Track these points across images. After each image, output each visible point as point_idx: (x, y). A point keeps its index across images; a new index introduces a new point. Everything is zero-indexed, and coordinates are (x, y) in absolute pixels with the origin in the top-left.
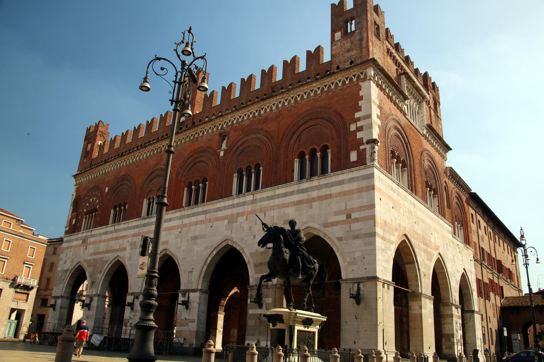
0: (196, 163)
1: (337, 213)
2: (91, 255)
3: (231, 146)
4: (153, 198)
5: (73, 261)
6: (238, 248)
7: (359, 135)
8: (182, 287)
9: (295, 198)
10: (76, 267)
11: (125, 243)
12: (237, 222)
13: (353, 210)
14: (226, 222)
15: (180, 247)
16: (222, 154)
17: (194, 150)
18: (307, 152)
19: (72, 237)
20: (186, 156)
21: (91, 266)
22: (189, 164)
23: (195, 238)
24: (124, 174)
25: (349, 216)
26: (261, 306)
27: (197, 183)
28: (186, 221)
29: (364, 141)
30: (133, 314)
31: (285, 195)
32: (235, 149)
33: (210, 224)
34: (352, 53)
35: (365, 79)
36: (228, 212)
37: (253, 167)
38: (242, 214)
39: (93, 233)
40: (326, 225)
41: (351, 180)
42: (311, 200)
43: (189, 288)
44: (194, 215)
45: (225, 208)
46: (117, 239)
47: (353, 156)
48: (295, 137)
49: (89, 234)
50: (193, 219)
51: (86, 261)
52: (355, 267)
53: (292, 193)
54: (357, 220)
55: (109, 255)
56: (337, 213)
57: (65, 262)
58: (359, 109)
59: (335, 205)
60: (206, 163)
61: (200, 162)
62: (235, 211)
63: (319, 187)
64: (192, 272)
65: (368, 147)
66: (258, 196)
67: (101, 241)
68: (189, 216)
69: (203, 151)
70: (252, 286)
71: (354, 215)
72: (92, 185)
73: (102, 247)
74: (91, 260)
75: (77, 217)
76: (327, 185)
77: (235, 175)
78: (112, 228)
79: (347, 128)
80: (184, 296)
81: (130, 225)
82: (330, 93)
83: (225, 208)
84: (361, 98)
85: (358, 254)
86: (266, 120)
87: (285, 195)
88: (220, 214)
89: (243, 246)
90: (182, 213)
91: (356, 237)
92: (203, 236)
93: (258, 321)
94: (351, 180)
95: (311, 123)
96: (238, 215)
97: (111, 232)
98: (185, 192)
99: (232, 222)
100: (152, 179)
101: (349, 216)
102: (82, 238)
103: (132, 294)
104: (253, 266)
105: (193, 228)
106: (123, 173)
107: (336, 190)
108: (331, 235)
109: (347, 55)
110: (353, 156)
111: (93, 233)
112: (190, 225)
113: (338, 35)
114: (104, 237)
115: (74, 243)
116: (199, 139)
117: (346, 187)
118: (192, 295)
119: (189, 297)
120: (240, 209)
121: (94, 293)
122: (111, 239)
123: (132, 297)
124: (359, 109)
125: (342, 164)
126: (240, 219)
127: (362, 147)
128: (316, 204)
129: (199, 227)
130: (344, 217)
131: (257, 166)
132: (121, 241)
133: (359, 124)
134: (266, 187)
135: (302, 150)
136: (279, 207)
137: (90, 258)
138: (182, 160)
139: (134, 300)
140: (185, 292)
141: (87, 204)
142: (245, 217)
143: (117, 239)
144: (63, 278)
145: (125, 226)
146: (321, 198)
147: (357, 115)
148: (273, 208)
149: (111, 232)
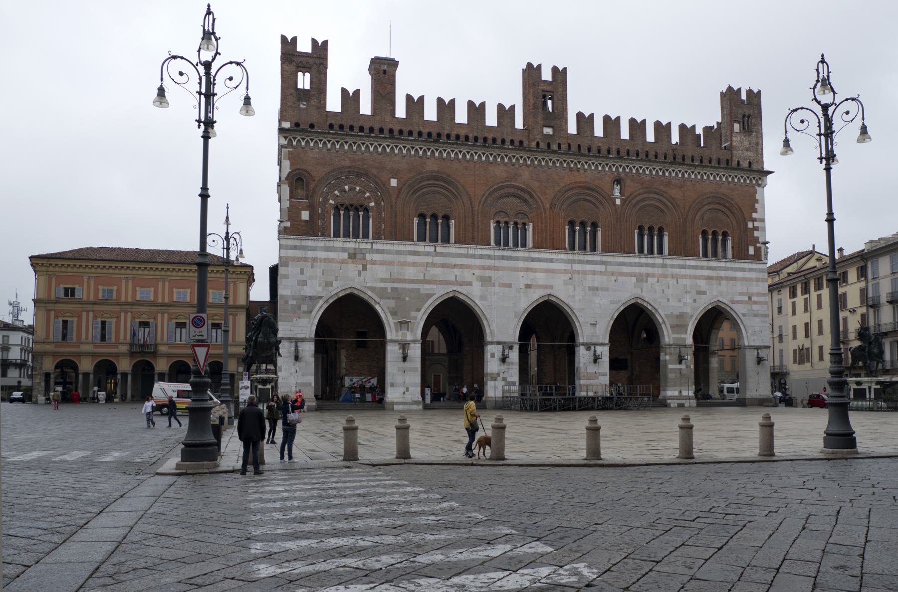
0: (579, 200)
1: (741, 294)
2: (383, 280)
3: (628, 197)
4: (507, 223)
5: (328, 284)
6: (650, 308)
7: (756, 234)
8: (581, 339)
9: (706, 273)
10: (341, 295)
11: (467, 275)
12: (647, 281)
13: (753, 294)
14: (634, 279)
15: (574, 296)
16: (618, 202)
17: (576, 183)
18: (710, 232)
19: (310, 243)
20: (562, 185)
21: (389, 298)
22: (569, 198)
23: (594, 289)
24: (435, 168)
25: (750, 298)
26: (680, 363)
27: (583, 224)
28: (577, 267)
29: (761, 240)
30: (504, 367)
31: (696, 267)
32: (634, 202)
33: (613, 278)
34: (751, 154)
35: (759, 185)
36: (636, 270)
37: (656, 229)
38: (653, 276)
39: (375, 246)
40: (733, 302)
41: (751, 270)
42: (720, 279)
43: (594, 341)
44: (588, 262)
45: (630, 264)
46: (443, 266)
47: (751, 251)
48: (699, 214)
49: (369, 246)
50: (588, 267)
51: (372, 289)
52: (755, 338)
53: (702, 268)
54: (755, 303)
55: (434, 286)
56: (741, 294)
57: (304, 283)
58: (756, 211)
59: (740, 287)
60: (595, 205)
61: (585, 200)
62: (644, 270)
63: (726, 269)
64: (595, 325)
65: (763, 246)
66: (668, 262)
67: (404, 264)
68: (580, 262)
69: (593, 190)
70: (670, 345)
71: (754, 299)
72: (347, 163)
73: (410, 273)
74: (386, 288)
75: (311, 208)
76: (732, 269)
77: (636, 231)
78: (432, 249)
79: (747, 225)
80: (588, 349)
81: (471, 252)
82: (731, 185)
83: (630, 264)
84: (757, 201)
85: (757, 329)
86: (669, 184)
87: (696, 267)
88: (625, 269)
89: (656, 307)
90: (570, 257)
91: (756, 315)
92: (607, 289)
93: (678, 375)
94: (751, 270)
95: (716, 206)
96: (648, 275)
97: (428, 254)
98: (567, 231)
99: (642, 281)
100: (501, 197)
101: (750, 298)
102: (344, 250)
103: (499, 343)
104: (669, 327)
105: (589, 277)
106: (431, 166)
107: (739, 274)
108: (739, 310)
109: (745, 153)
110: (751, 251)
111: (375, 246)
112: (585, 273)
113: (737, 127)
114: (411, 259)
115: (322, 255)
116: (582, 171)
117: (747, 275)
118: (599, 349)
119: (595, 351)
120: (650, 270)
121: (409, 337)
122: (434, 265)
123: (501, 347)
124: (756, 211)
125: (740, 254)
126: (650, 279)
127: (758, 245)
128: (724, 282)
129: (598, 278)
130: (746, 298)
131: (661, 230)
132: (457, 271)
133: (756, 224)
134: (675, 254)
135: (705, 228)
136: (691, 277)
137: (382, 285)
138: (557, 188)
139: (504, 351)
140: (588, 346)
141: (336, 192)
142: (656, 279)
143: (443, 266)
144: (304, 308)
145: (463, 251)
146: (728, 279)
147: (754, 215)
148: (685, 277)
149: (428, 254)
